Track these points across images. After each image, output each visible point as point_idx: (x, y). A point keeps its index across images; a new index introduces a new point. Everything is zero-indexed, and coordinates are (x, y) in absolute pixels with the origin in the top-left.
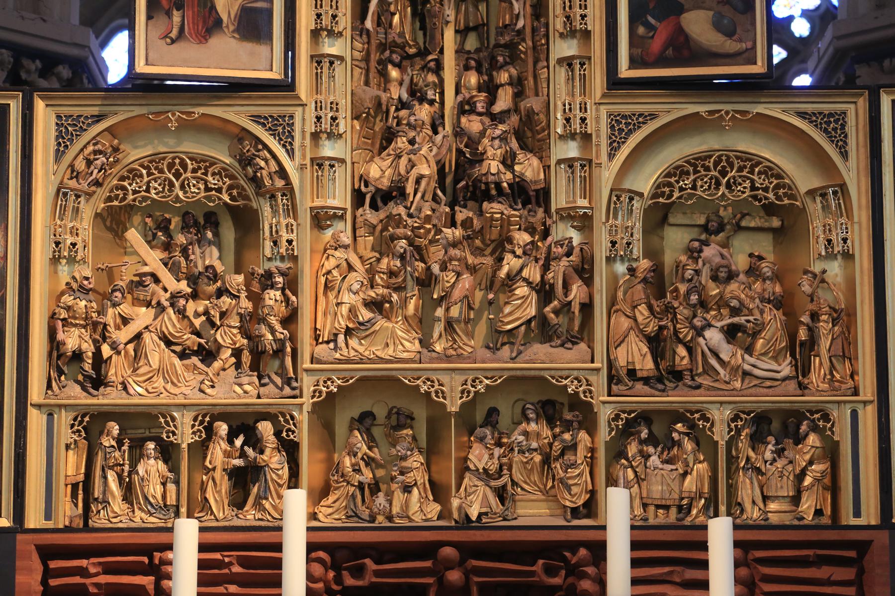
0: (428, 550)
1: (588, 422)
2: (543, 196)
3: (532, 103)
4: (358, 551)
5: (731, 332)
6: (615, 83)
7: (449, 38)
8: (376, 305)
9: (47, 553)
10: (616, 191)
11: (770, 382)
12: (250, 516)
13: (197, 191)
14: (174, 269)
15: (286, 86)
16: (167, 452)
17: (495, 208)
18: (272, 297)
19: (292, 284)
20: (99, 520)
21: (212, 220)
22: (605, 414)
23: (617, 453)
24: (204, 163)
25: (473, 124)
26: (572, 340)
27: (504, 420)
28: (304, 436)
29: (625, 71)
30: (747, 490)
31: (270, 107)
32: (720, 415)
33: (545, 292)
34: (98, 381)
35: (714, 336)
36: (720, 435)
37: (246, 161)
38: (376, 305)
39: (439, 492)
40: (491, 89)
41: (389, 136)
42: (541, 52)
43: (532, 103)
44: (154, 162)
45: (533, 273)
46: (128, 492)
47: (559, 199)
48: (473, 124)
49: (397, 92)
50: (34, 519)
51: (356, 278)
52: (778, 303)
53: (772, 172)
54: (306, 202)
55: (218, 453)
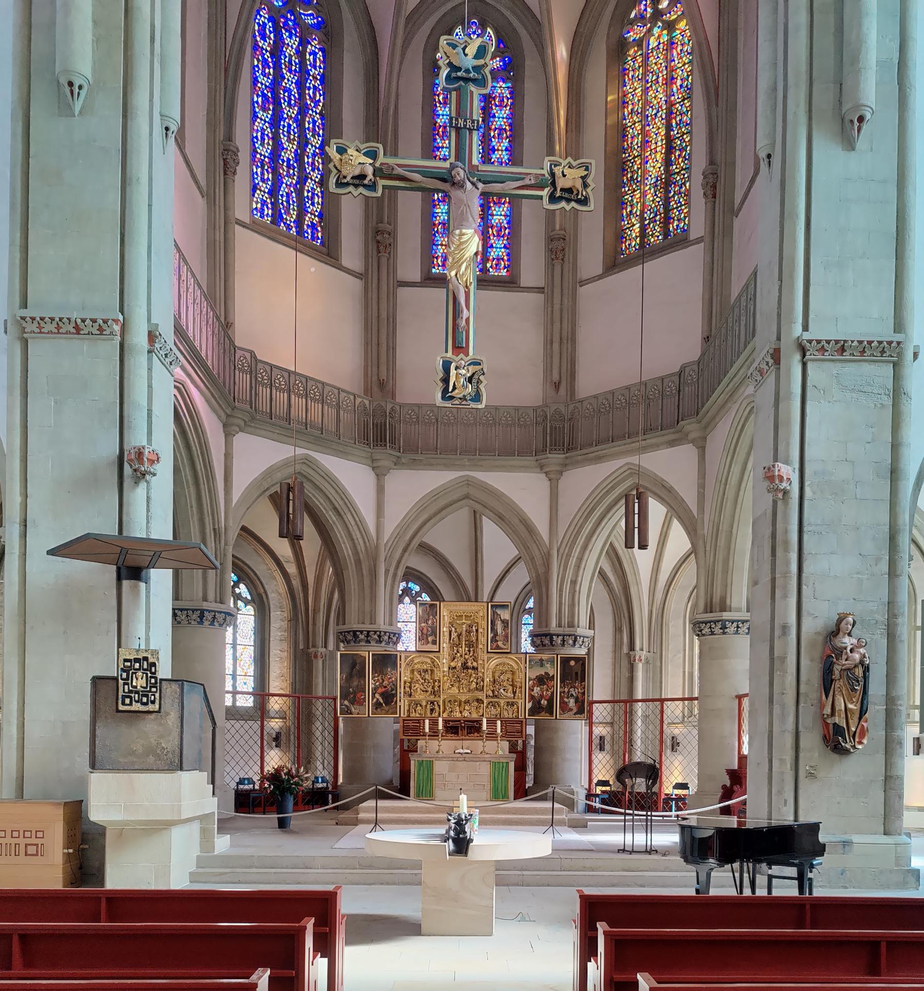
0: (459, 721)
1: (483, 703)
2: (477, 668)
3: (476, 655)
4: (449, 721)
5: (504, 690)
6: (488, 652)
7: (464, 643)
8: (452, 685)
9: (404, 720)
10: (488, 669)
11: (510, 698)
12: (433, 715)
13: (425, 667)
14: (422, 679)
15: (439, 651)
16: (421, 705)
17: (470, 671)
18: (436, 683)
19: (439, 681)
20: (411, 715)
21: (427, 670)
22: (485, 702)
23: (487, 707)
24: (426, 663)
25: (467, 657)
26: (480, 691)
27: (471, 702)
28: (441, 704)
29: (489, 650)
30: (506, 713)
31: (436, 654)
32: (502, 702)
33: (477, 684)
34: (410, 695)
35: (502, 690)
36: (502, 705)
37: (433, 663)
38: (452, 685)
39: (461, 712)
40: (469, 651)
41: (454, 659)
42: (477, 647)
43: (476, 655)
44: (418, 663)
45: (475, 680)
46: (415, 712)
47: (479, 670)
48: (467, 657)
49: (455, 651)
50: (402, 715)
51: (449, 681)
52: (512, 685)
53: (511, 665)
54: (442, 670)
55: (428, 706)
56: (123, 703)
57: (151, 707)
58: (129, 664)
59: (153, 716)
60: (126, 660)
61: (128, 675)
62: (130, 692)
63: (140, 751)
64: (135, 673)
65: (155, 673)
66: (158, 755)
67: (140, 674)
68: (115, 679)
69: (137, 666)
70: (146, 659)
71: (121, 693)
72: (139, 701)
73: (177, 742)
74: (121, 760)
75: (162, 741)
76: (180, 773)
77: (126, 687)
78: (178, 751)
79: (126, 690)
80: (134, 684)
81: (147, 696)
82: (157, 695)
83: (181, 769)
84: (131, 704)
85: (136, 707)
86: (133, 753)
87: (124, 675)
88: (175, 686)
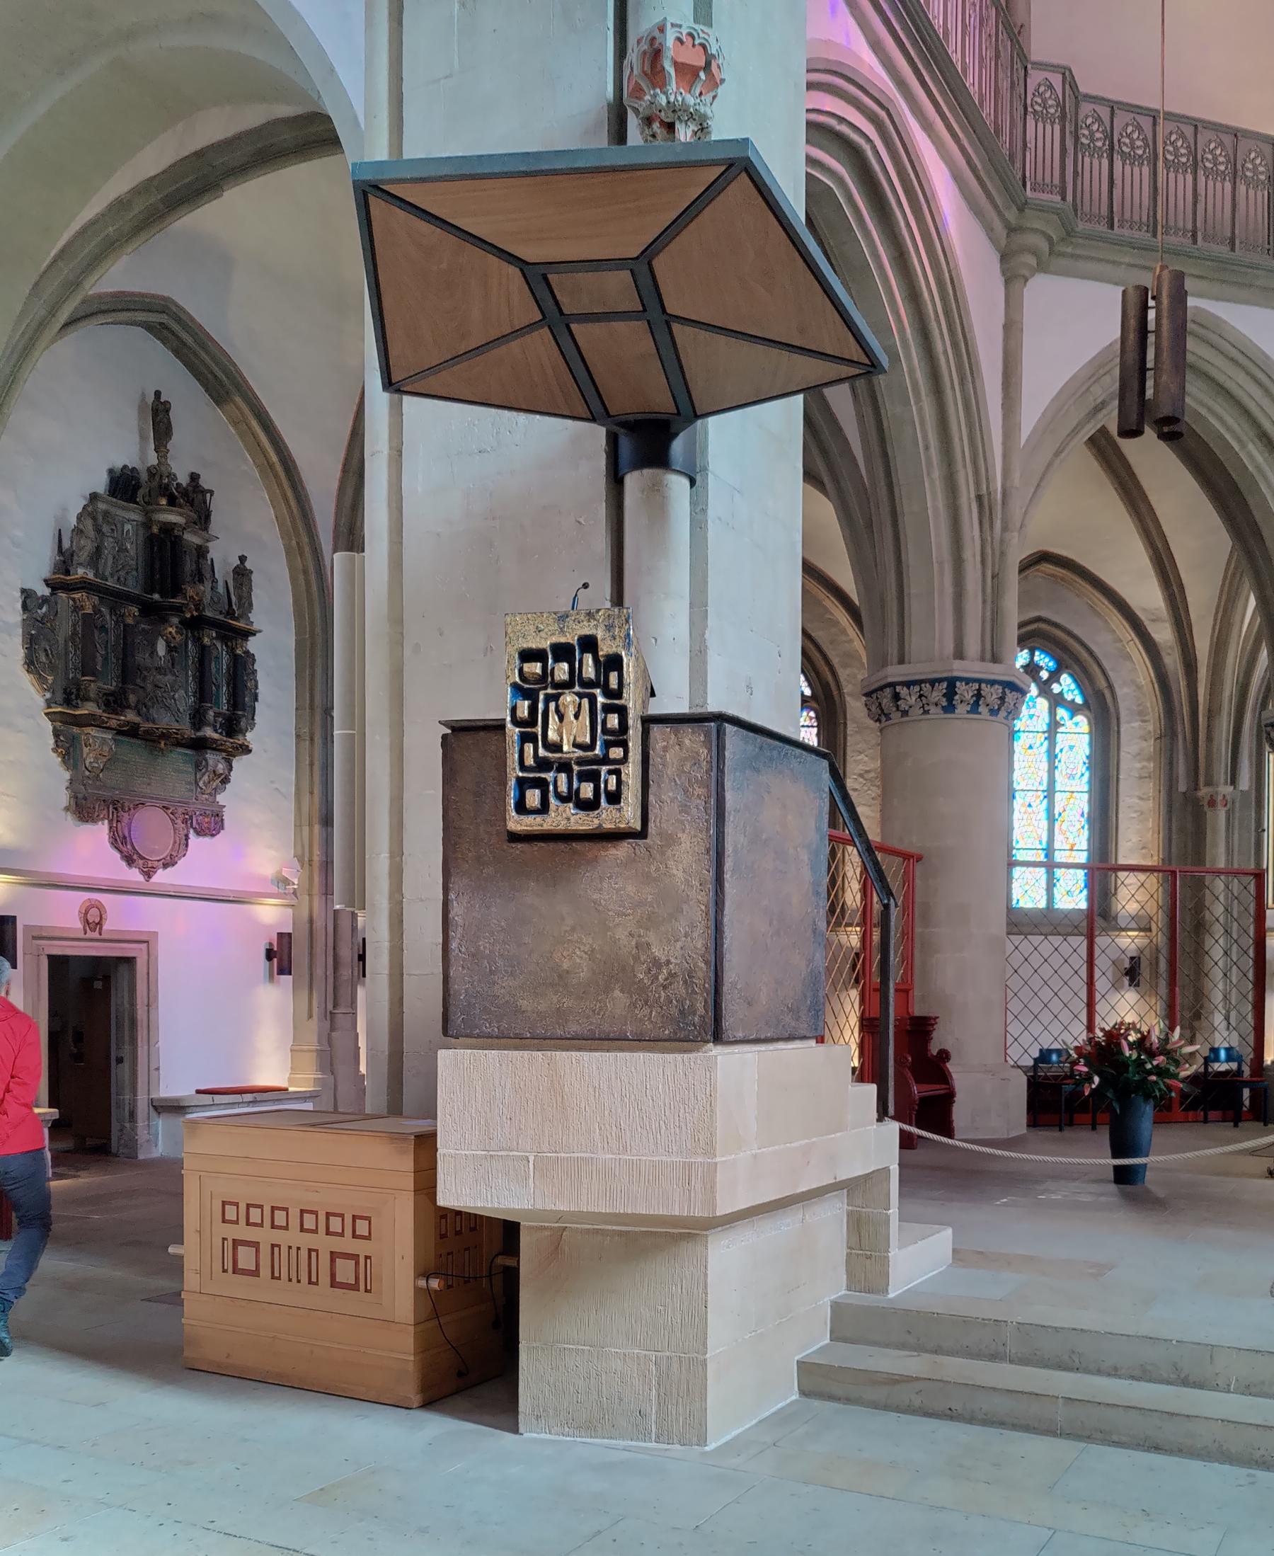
56: (521, 808)
57: (606, 817)
58: (537, 668)
59: (622, 850)
60: (528, 656)
61: (533, 709)
62: (543, 765)
63: (584, 975)
64: (556, 698)
65: (618, 694)
66: (642, 989)
67: (569, 699)
68: (499, 727)
69: (562, 671)
70: (589, 644)
71: (514, 772)
72: (571, 797)
73: (699, 941)
74: (524, 1004)
75: (651, 937)
76: (715, 1051)
77: (529, 748)
78: (703, 970)
79: (530, 761)
80: (552, 735)
81: (593, 777)
82: (631, 772)
83: (718, 1037)
84: (544, 808)
85: (563, 817)
86: (561, 979)
87: (524, 708)
88: (692, 739)
